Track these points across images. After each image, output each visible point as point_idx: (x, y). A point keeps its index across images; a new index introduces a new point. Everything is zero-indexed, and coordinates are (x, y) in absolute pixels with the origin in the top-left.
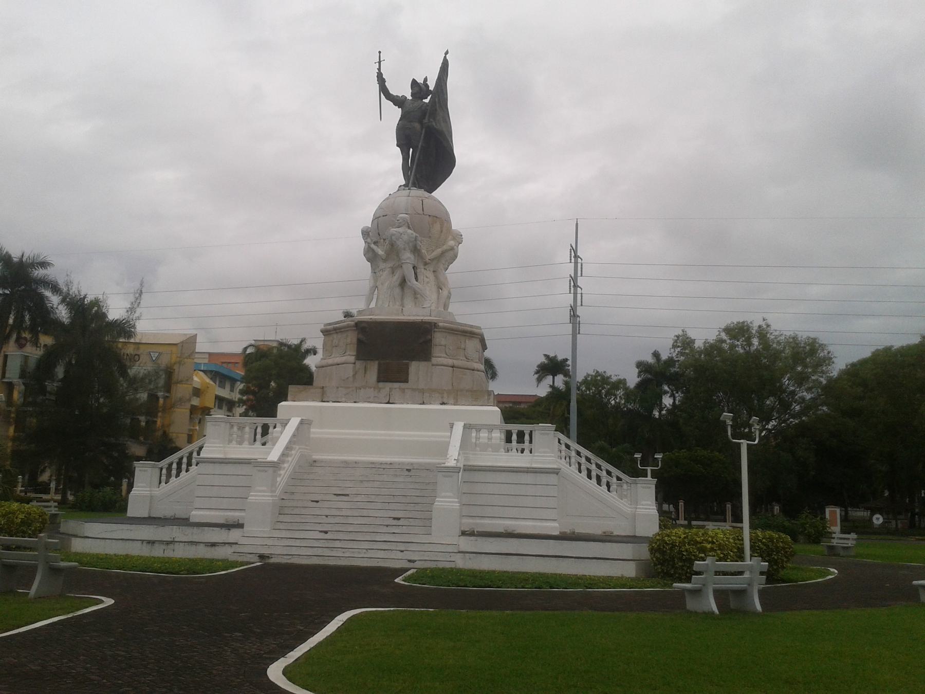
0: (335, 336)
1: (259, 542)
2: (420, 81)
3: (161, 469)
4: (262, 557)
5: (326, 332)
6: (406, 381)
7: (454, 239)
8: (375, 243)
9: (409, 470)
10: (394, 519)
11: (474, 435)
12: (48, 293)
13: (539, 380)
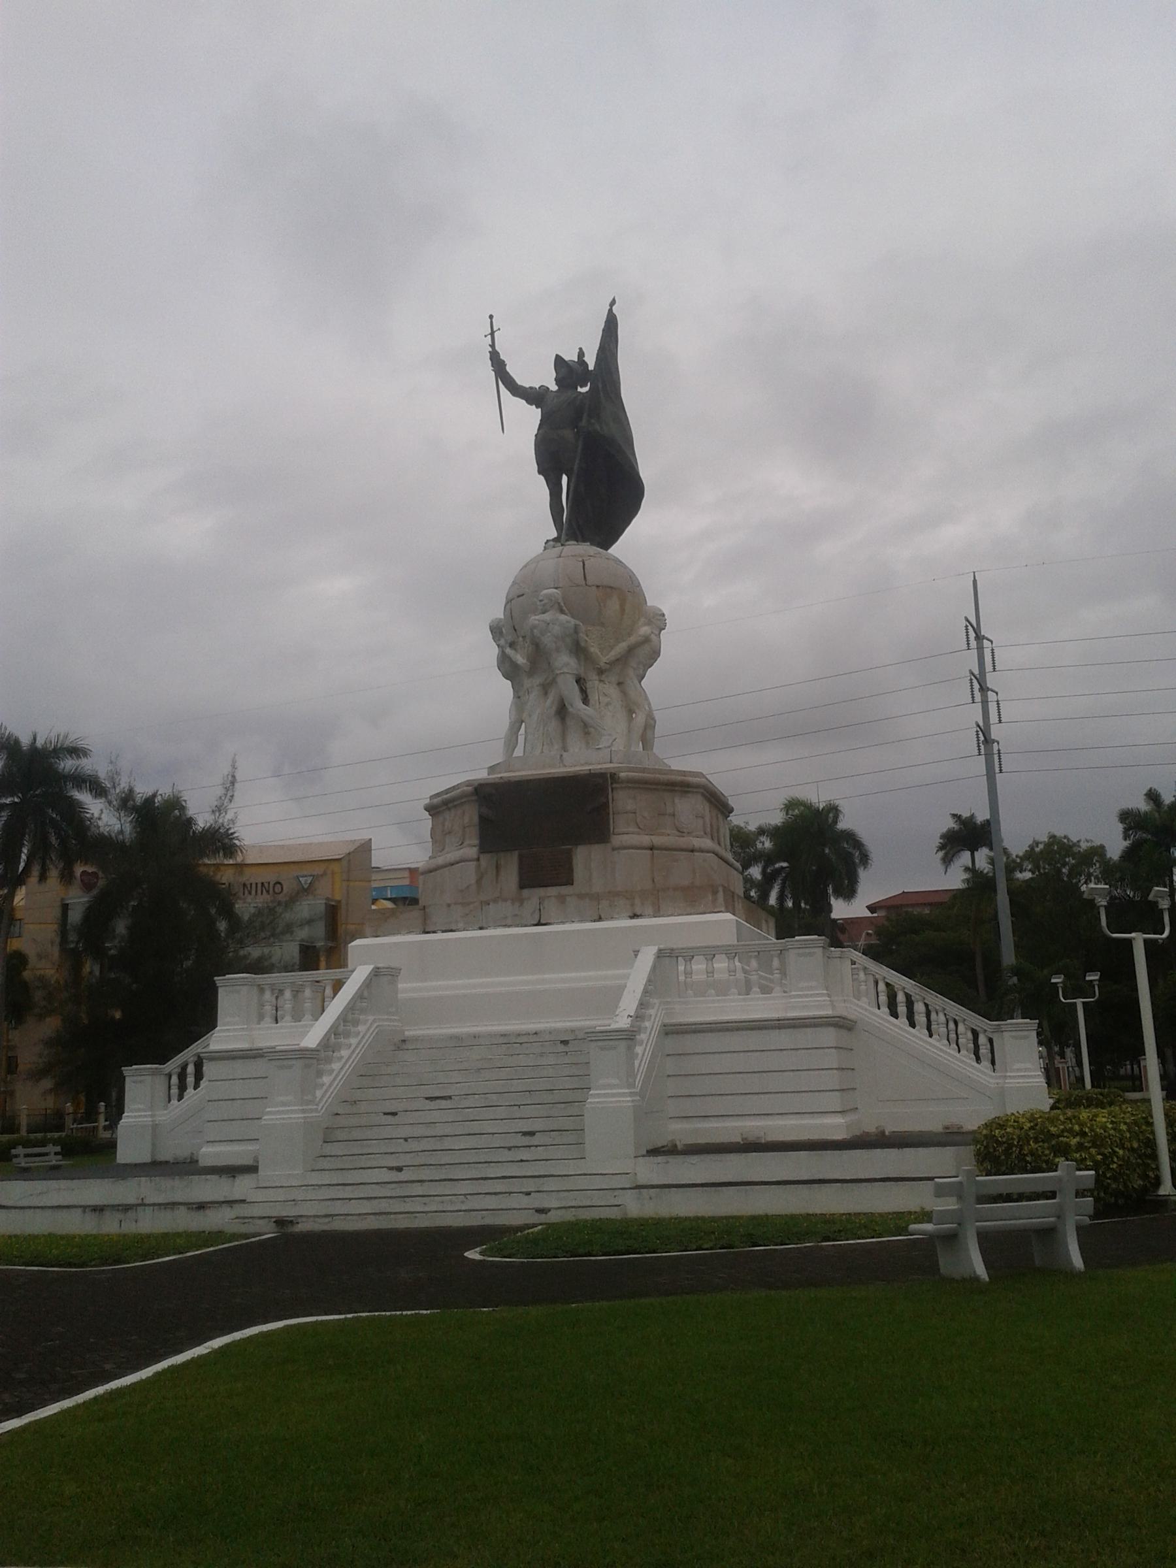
1: (281, 1195)
2: (571, 356)
3: (170, 1076)
4: (281, 1222)
5: (434, 810)
6: (570, 882)
7: (649, 623)
8: (512, 645)
9: (565, 1042)
10: (525, 1134)
11: (681, 968)
12: (83, 797)
13: (947, 861)
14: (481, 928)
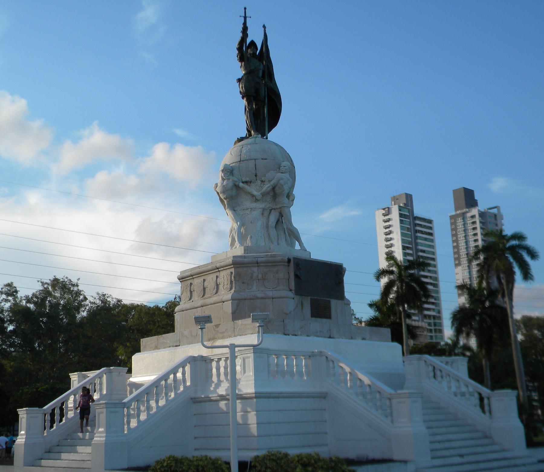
0: (255, 269)
14: (308, 336)
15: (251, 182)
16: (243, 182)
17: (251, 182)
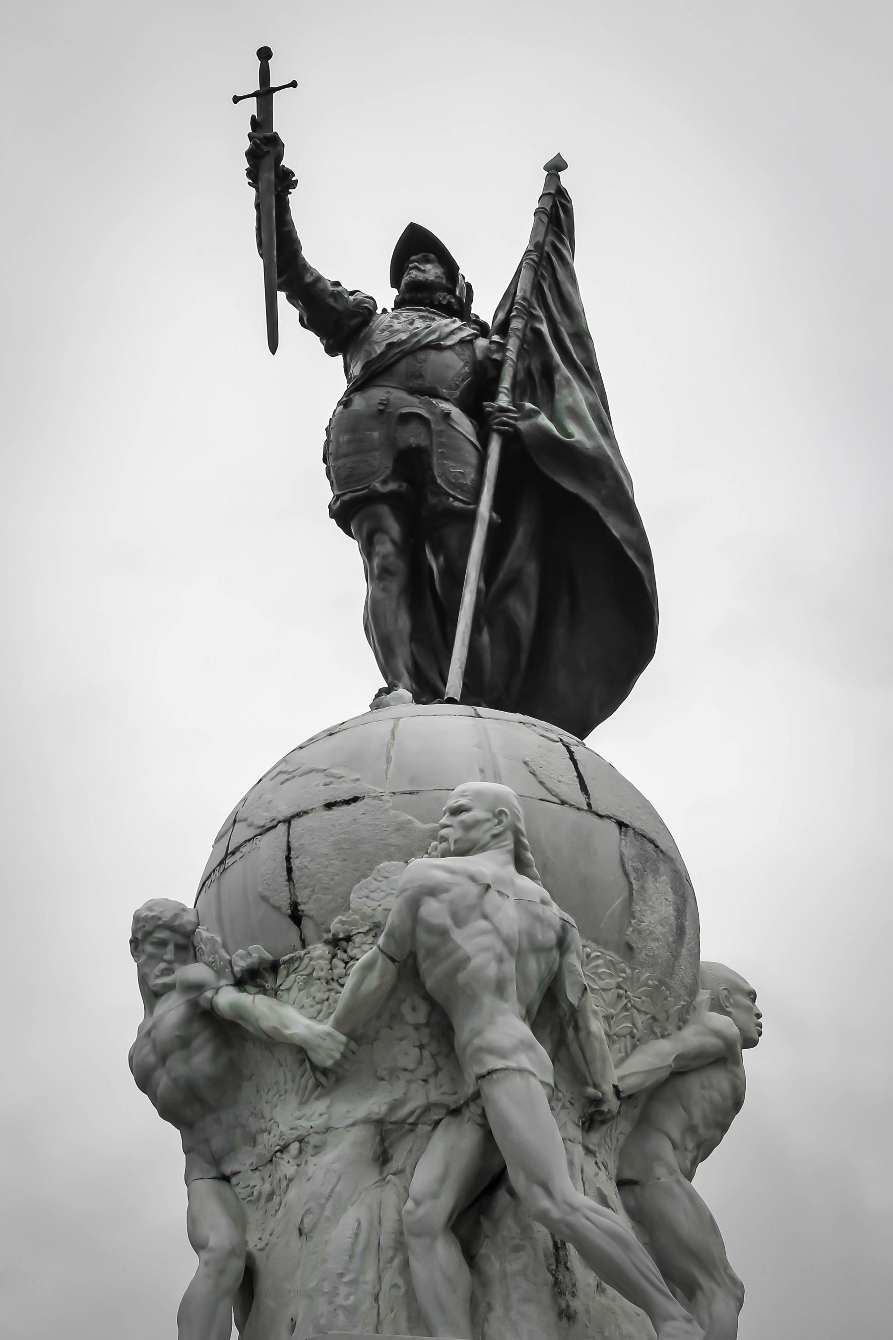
15: (274, 967)
16: (240, 983)
17: (274, 967)
